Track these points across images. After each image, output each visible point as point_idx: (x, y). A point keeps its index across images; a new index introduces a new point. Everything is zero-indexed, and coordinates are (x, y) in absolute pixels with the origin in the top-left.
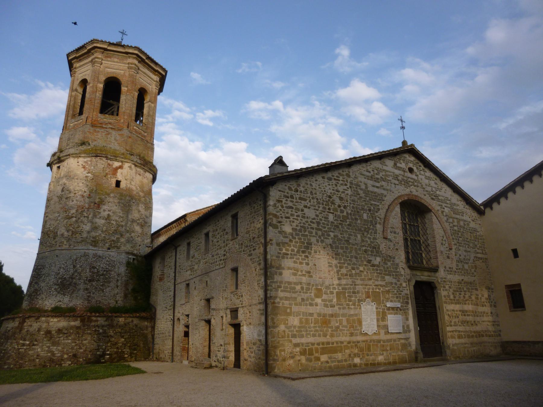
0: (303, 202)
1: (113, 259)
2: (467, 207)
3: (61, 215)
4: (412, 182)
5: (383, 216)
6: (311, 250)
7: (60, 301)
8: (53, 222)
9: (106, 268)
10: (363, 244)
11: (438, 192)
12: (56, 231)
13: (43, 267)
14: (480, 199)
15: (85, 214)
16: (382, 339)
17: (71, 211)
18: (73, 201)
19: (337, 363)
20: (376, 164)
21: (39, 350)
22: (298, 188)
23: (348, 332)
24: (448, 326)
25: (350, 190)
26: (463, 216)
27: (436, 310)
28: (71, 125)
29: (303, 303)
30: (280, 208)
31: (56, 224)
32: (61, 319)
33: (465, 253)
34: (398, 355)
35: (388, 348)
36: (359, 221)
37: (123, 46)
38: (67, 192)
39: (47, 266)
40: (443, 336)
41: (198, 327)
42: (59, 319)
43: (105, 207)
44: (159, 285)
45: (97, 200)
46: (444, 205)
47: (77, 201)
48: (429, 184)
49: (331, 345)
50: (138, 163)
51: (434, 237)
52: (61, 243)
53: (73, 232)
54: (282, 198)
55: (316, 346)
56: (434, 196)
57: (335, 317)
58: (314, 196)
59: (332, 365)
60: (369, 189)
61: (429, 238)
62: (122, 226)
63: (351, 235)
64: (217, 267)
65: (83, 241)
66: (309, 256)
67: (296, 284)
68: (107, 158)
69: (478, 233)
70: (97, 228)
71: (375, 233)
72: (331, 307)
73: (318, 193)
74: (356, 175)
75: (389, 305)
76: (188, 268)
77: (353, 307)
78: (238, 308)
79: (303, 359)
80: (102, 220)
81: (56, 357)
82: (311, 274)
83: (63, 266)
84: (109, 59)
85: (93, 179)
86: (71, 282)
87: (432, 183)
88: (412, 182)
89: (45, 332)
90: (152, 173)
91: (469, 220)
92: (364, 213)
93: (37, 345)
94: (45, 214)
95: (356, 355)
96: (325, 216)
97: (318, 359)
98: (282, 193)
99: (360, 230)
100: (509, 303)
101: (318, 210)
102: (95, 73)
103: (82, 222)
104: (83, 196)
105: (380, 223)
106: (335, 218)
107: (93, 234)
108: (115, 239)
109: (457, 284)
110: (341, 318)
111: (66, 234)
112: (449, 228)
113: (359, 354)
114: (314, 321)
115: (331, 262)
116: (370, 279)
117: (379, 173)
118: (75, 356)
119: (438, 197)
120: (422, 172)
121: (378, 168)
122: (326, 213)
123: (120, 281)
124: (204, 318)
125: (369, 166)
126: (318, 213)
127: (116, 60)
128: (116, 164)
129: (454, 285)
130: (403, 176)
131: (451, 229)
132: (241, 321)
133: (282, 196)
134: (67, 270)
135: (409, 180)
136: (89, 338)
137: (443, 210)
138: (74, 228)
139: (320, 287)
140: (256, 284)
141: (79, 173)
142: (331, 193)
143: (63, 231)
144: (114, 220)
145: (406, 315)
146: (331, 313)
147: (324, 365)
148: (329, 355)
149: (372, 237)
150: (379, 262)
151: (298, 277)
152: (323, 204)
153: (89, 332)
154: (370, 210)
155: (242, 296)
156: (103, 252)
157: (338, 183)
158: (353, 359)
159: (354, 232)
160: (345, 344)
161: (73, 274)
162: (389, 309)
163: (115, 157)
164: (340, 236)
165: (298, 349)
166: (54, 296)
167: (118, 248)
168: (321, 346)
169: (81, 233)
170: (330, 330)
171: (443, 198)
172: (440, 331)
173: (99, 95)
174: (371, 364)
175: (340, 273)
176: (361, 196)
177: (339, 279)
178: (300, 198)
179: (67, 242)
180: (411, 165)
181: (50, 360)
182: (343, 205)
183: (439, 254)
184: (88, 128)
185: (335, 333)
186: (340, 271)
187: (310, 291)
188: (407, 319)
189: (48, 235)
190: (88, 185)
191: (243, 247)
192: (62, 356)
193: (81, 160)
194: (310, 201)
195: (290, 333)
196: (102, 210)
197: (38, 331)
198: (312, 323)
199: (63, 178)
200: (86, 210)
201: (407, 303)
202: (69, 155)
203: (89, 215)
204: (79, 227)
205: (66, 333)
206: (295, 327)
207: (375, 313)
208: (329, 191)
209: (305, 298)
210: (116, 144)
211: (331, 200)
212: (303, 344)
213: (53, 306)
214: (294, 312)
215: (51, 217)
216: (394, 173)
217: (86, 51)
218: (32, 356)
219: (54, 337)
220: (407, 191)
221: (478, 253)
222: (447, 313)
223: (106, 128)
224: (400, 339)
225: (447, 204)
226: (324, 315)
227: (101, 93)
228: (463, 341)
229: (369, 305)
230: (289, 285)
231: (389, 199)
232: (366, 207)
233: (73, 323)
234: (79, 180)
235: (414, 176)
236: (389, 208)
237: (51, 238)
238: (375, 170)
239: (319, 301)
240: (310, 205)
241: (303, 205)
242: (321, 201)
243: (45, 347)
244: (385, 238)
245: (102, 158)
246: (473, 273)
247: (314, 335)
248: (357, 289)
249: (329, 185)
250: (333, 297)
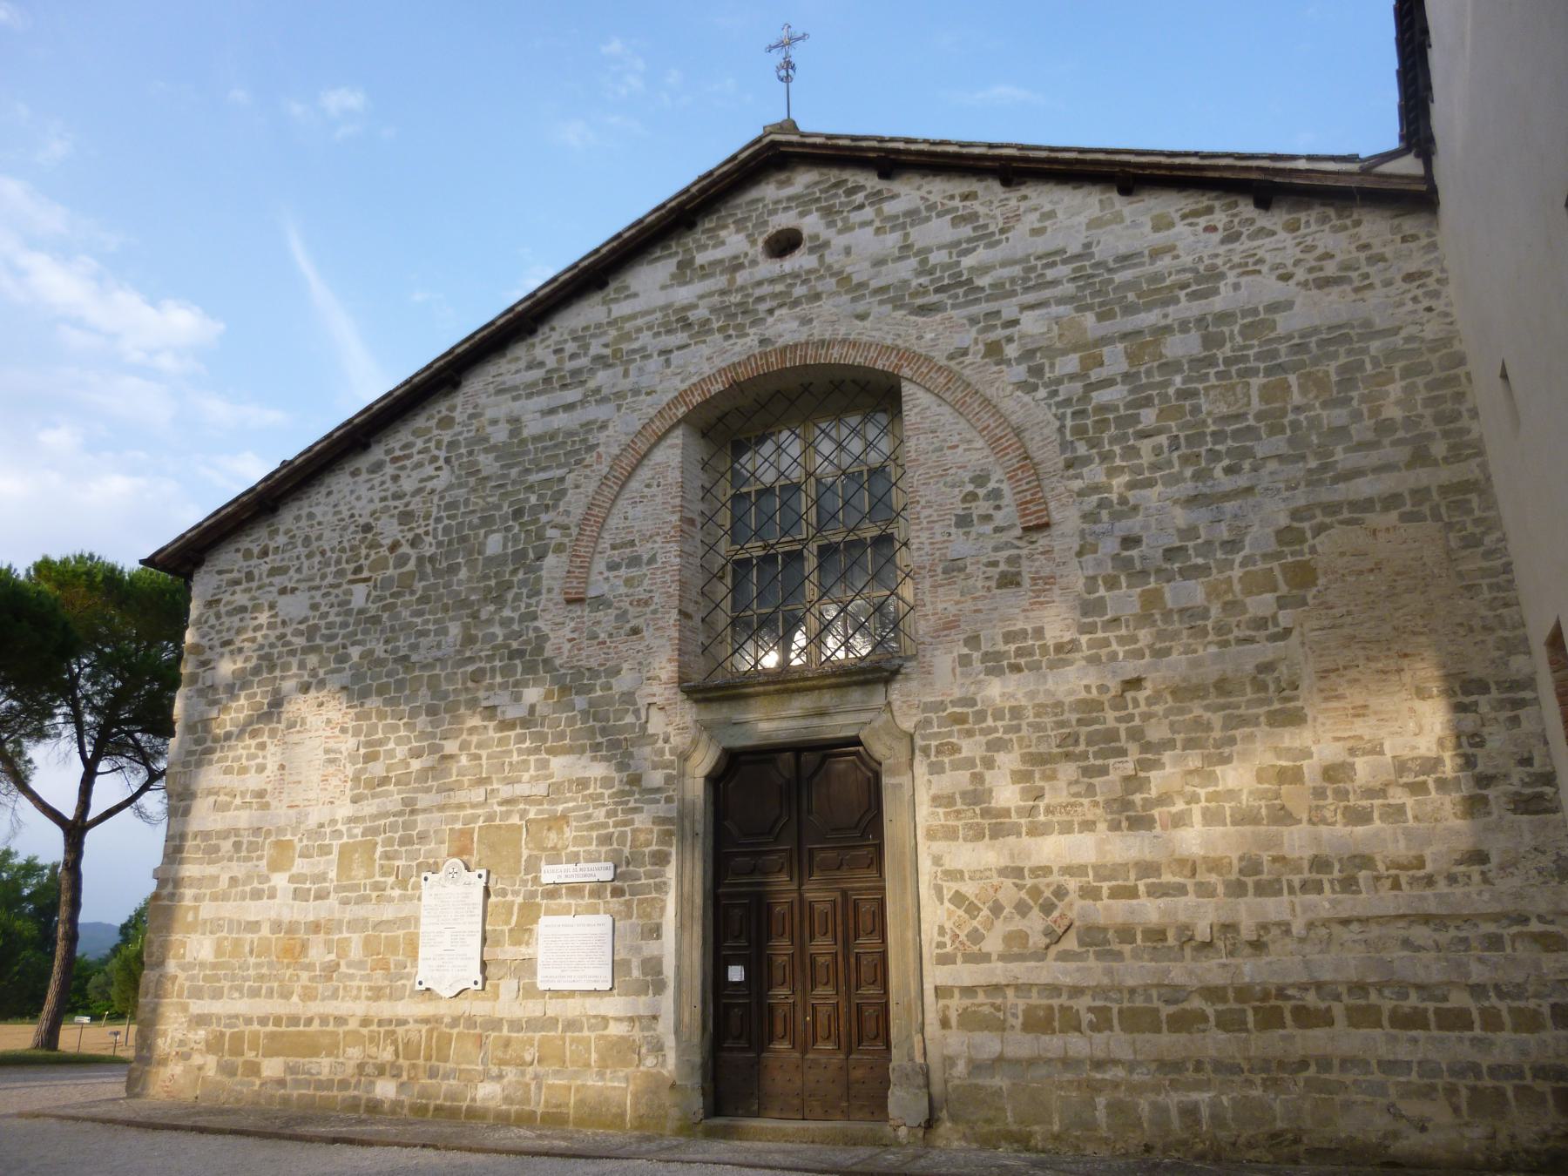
0: (277, 580)
6: (279, 722)
10: (468, 654)
16: (506, 1015)
19: (311, 1092)
30: (213, 621)
34: (577, 1090)
36: (463, 573)
49: (301, 1028)
59: (295, 1093)
60: (526, 433)
67: (225, 835)
72: (317, 898)
75: (551, 874)
77: (397, 892)
79: (211, 1062)
95: (381, 1070)
96: (342, 597)
97: (254, 1069)
101: (318, 588)
106: (374, 593)
110: (345, 935)
113: (400, 1068)
115: (335, 746)
116: (482, 781)
117: (586, 347)
119: (970, 281)
126: (318, 595)
135: (758, 292)
139: (289, 837)
146: (311, 918)
147: (269, 1090)
148: (292, 1060)
158: (372, 1083)
159: (436, 622)
160: (353, 1025)
162: (553, 892)
165: (202, 1033)
168: (270, 1028)
174: (438, 1109)
176: (484, 474)
177: (355, 800)
178: (274, 572)
185: (320, 986)
186: (363, 770)
188: (655, 932)
194: (299, 570)
198: (251, 952)
206: (202, 965)
209: (240, 876)
211: (370, 536)
212: (219, 1019)
214: (205, 922)
222: (950, 888)
224: (605, 1020)
225: (1054, 283)
226: (292, 928)
239: (280, 880)
247: (254, 993)
248: (420, 827)
250: (328, 863)
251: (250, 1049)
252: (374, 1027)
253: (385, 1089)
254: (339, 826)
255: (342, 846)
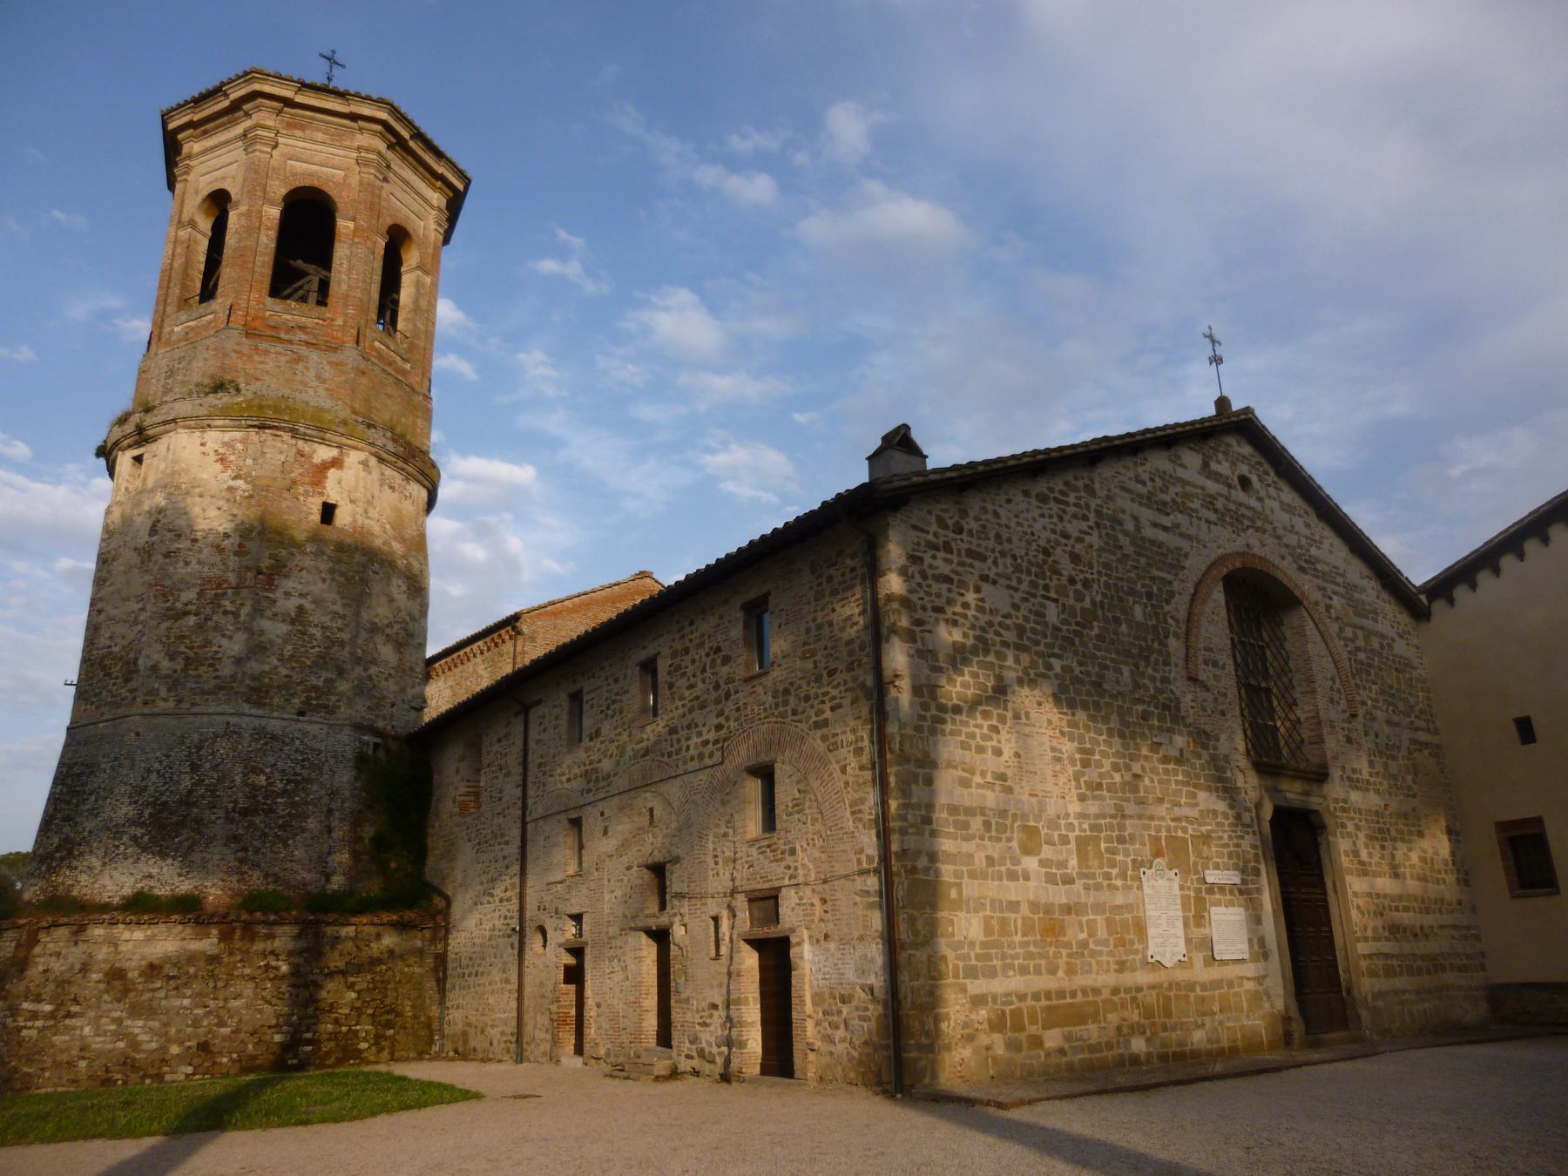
0: (977, 564)
1: (316, 746)
2: (1384, 595)
3: (148, 607)
4: (1250, 519)
5: (1182, 615)
7: (150, 876)
8: (121, 629)
9: (295, 774)
10: (1137, 696)
11: (1313, 551)
12: (132, 655)
13: (91, 768)
14: (1419, 571)
15: (227, 603)
17: (182, 594)
18: (187, 564)
19: (1087, 1055)
20: (1158, 461)
21: (87, 1030)
22: (963, 522)
23: (1111, 959)
24: (1358, 940)
25: (1095, 533)
26: (1376, 621)
27: (1325, 893)
28: (176, 329)
29: (990, 870)
31: (131, 635)
32: (156, 931)
33: (1387, 729)
35: (1216, 1008)
36: (1124, 628)
37: (342, 95)
38: (169, 535)
39: (103, 766)
40: (1347, 971)
41: (619, 952)
42: (149, 933)
43: (289, 584)
44: (458, 825)
45: (265, 563)
46: (1330, 587)
47: (199, 562)
48: (1292, 526)
49: (1069, 1000)
50: (389, 452)
51: (1310, 681)
52: (149, 693)
53: (187, 659)
54: (923, 549)
55: (1030, 1002)
56: (1306, 561)
57: (1077, 915)
58: (1006, 546)
61: (1295, 683)
62: (342, 644)
63: (1106, 667)
64: (694, 765)
65: (221, 688)
66: (1000, 727)
68: (294, 433)
69: (1414, 673)
70: (265, 648)
71: (1167, 663)
72: (1064, 883)
73: (1015, 538)
74: (1109, 490)
76: (577, 771)
77: (1119, 883)
78: (779, 889)
79: (998, 1040)
80: (281, 625)
81: (144, 1051)
82: (1009, 783)
83: (157, 765)
84: (298, 133)
85: (251, 497)
86: (185, 817)
87: (1299, 523)
88: (1250, 519)
89: (106, 974)
90: (427, 483)
91: (1392, 633)
92: (1135, 602)
93: (81, 1015)
94: (92, 605)
96: (1037, 608)
97: (1037, 1042)
98: (919, 533)
99: (1128, 653)
100: (1507, 874)
101: (1016, 590)
102: (256, 172)
103: (217, 628)
104: (219, 549)
105: (1176, 636)
107: (254, 666)
108: (321, 684)
109: (1375, 818)
110: (1091, 917)
111: (166, 665)
112: (1345, 655)
113: (1143, 1026)
114: (1023, 925)
115: (1058, 746)
118: (204, 1047)
119: (1313, 564)
120: (1272, 491)
121: (1164, 473)
122: (1040, 599)
123: (337, 814)
124: (641, 924)
125: (1142, 464)
127: (320, 136)
128: (323, 453)
129: (1367, 820)
130: (1227, 499)
131: (1350, 659)
132: (793, 930)
133: (923, 544)
134: (171, 778)
135: (1243, 511)
136: (248, 992)
137: (1328, 602)
138: (191, 648)
139: (1032, 823)
140: (848, 815)
141: (205, 476)
142: (1049, 541)
143: (157, 657)
144: (316, 626)
145: (1255, 909)
146: (1064, 901)
147: (1055, 1060)
149: (1158, 676)
150: (1181, 751)
151: (973, 790)
152: (1029, 573)
153: (247, 971)
154: (1149, 595)
155: (793, 852)
156: (284, 723)
157: (1065, 512)
158: (1128, 1042)
159: (1113, 660)
160: (1106, 994)
161: (190, 792)
162: (1211, 889)
163: (321, 429)
164: (1077, 670)
166: (131, 860)
167: (331, 711)
168: (1044, 1003)
169: (214, 662)
170: (1064, 952)
171: (1327, 568)
172: (1339, 955)
173: (267, 240)
174: (1174, 1054)
175: (1082, 780)
177: (1082, 798)
178: (971, 553)
179: (169, 690)
180: (1244, 469)
181: (124, 1064)
182: (1081, 576)
183: (1326, 730)
184: (234, 339)
185: (1078, 962)
186: (1083, 774)
187: (1008, 834)
188: (1258, 920)
189: (104, 668)
190: (235, 515)
191: (792, 699)
192: (163, 1048)
193: (214, 438)
194: (995, 563)
195: (961, 964)
196: (279, 594)
197: (80, 971)
199: (152, 491)
200: (229, 591)
201: (1257, 872)
202: (174, 421)
203: (239, 609)
204: (207, 643)
205: (173, 977)
206: (972, 944)
207: (1179, 901)
208: (1045, 535)
209: (996, 856)
210: (322, 392)
212: (994, 997)
213: (127, 891)
215: (112, 612)
216: (1203, 489)
217: (226, 103)
218: (62, 1051)
219: (135, 990)
220: (1239, 544)
221: (1418, 729)
223: (290, 342)
225: (1337, 584)
226: (1048, 909)
227: (273, 234)
228: (1398, 983)
229: (1162, 878)
230: (950, 815)
231: (1196, 564)
232: (1139, 585)
233: (194, 945)
234: (207, 500)
235: (1253, 502)
236: (1196, 590)
237: (117, 678)
238: (1157, 479)
239: (1031, 863)
240: (997, 574)
241: (976, 573)
242: (1025, 565)
243: (108, 1020)
244: (1193, 679)
245: (279, 433)
246: (1409, 788)
247: (1024, 970)
249: (1042, 515)
250: (1069, 851)
251: (1031, 1023)
252: (1122, 995)
253: (1138, 1045)
254: (1071, 820)
255: (1078, 838)
